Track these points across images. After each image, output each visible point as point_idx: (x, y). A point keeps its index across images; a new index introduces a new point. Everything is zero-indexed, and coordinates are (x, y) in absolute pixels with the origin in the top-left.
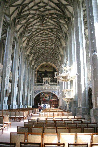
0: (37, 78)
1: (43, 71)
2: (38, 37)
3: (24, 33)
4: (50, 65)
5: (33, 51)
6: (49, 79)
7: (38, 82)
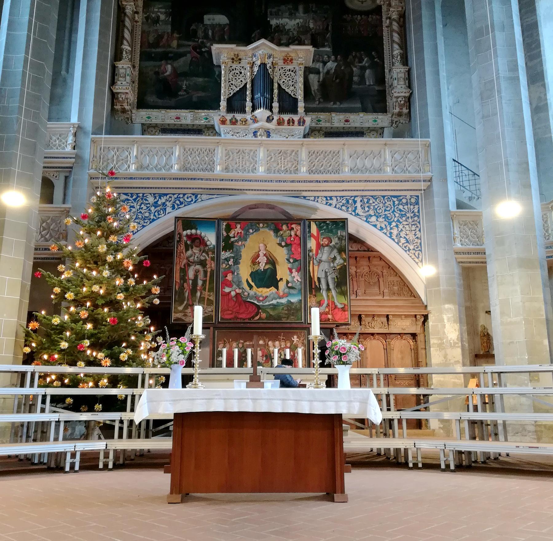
0: (145, 56)
6: (287, 60)
7: (151, 99)
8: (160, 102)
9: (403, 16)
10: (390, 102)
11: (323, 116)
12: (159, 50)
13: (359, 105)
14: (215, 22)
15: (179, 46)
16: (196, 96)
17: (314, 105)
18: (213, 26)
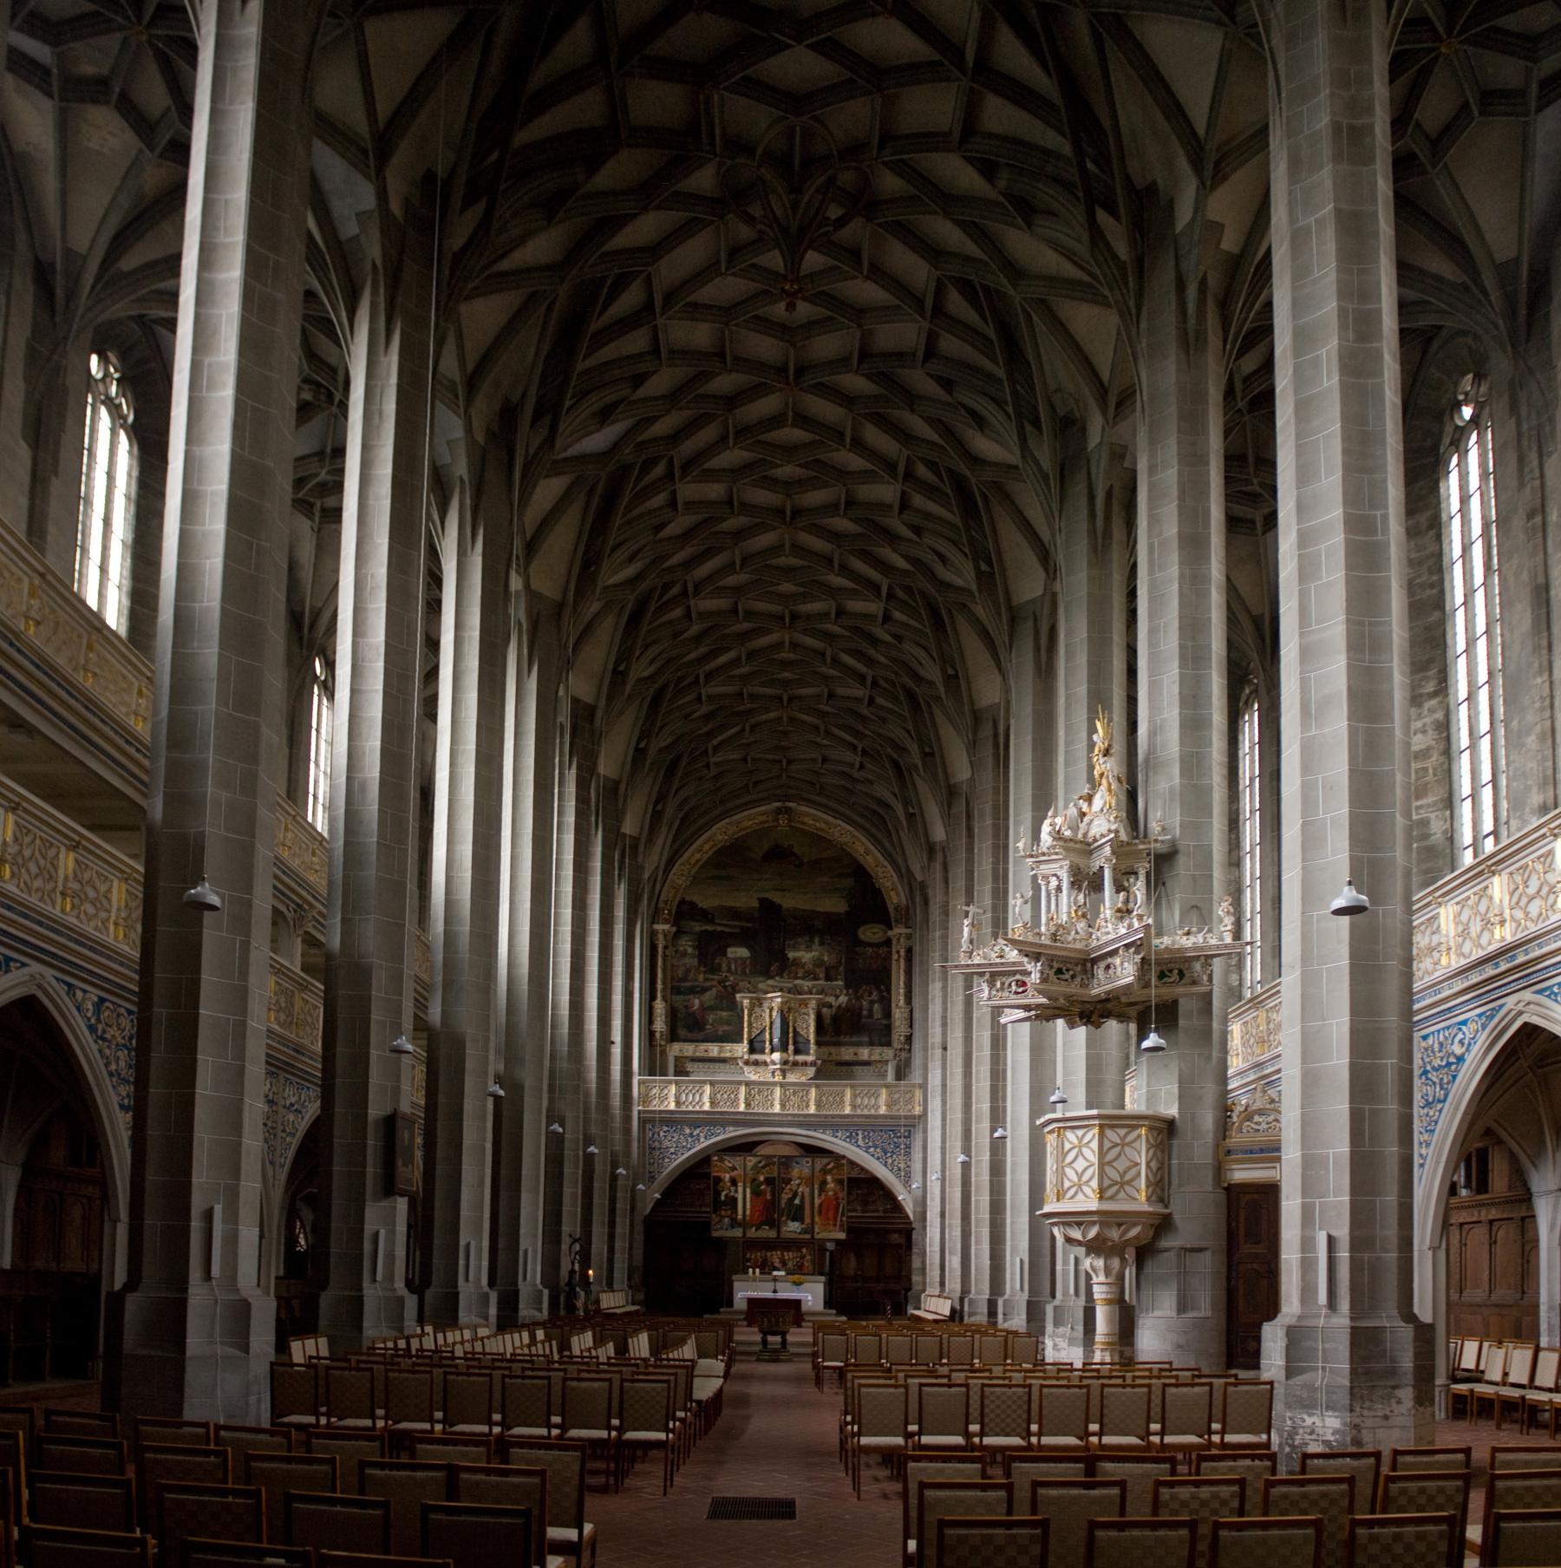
0: (676, 991)
1: (734, 914)
2: (712, 475)
3: (549, 410)
4: (818, 839)
5: (640, 669)
7: (682, 1032)
8: (690, 1035)
9: (909, 951)
10: (895, 1037)
11: (833, 1050)
12: (688, 984)
13: (866, 1039)
14: (738, 955)
15: (706, 980)
16: (722, 1029)
17: (825, 1039)
18: (735, 960)
